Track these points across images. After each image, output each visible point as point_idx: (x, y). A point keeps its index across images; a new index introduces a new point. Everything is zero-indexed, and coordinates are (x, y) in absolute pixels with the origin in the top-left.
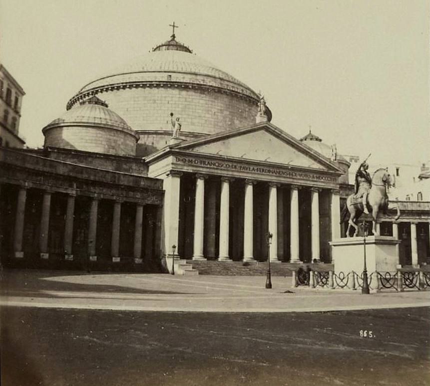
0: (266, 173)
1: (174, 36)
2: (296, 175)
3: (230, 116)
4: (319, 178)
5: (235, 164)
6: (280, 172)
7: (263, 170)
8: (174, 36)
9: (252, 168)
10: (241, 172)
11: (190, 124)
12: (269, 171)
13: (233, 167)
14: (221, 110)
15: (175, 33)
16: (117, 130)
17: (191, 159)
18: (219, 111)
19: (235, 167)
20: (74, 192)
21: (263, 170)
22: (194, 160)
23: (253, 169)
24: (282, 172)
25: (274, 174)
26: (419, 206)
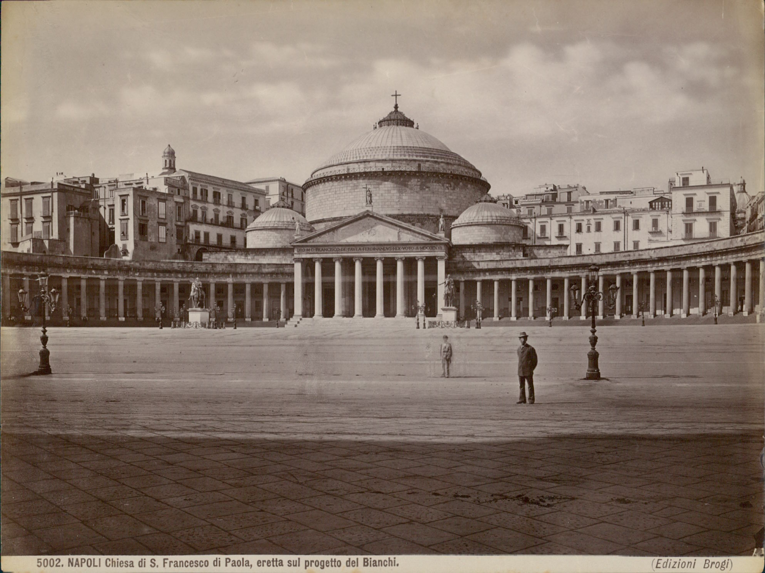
1: (396, 107)
2: (399, 248)
3: (398, 195)
4: (423, 248)
6: (384, 248)
7: (369, 249)
8: (396, 107)
9: (358, 248)
10: (349, 253)
11: (361, 208)
14: (388, 190)
15: (397, 103)
16: (282, 229)
17: (308, 248)
18: (387, 192)
20: (231, 280)
21: (369, 249)
22: (310, 248)
24: (387, 248)
25: (379, 251)
26: (523, 263)
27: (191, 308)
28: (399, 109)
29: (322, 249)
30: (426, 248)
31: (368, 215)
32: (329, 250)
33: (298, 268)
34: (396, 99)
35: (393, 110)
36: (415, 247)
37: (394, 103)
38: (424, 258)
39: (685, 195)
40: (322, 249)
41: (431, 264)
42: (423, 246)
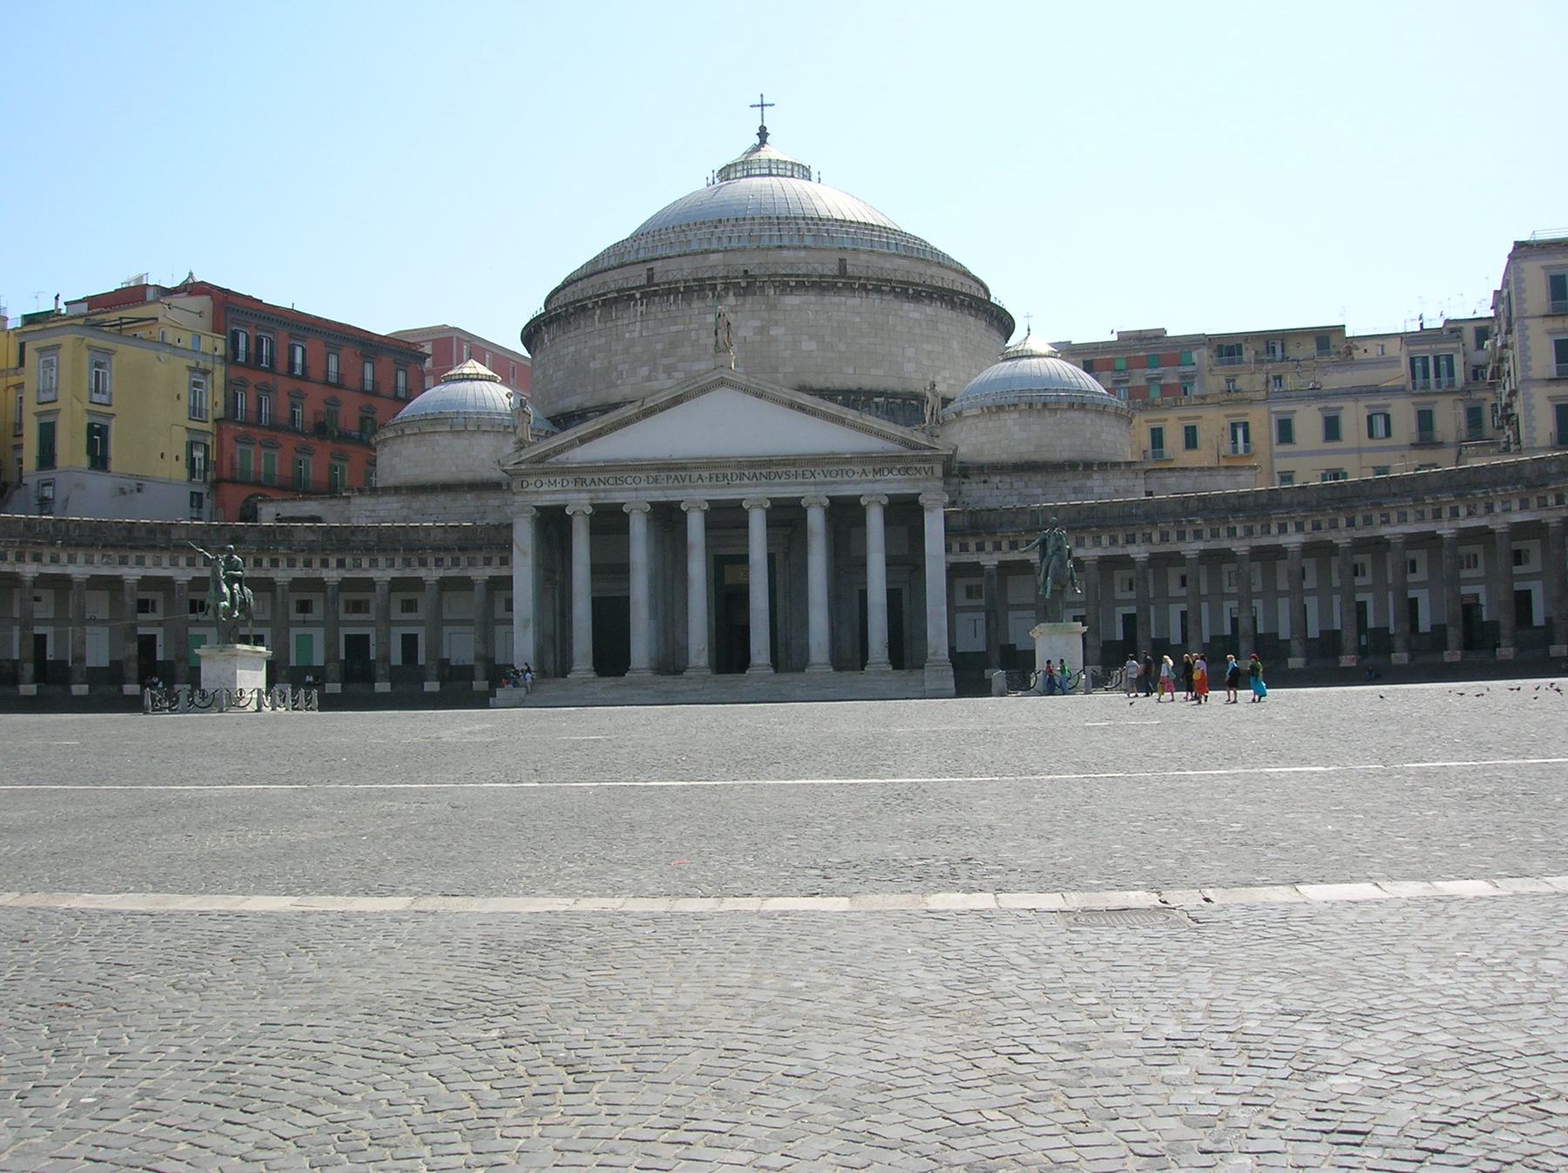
1: (763, 134)
4: (881, 471)
5: (654, 474)
8: (763, 134)
13: (651, 480)
19: (656, 480)
21: (725, 476)
22: (559, 480)
30: (890, 472)
31: (722, 383)
32: (611, 481)
33: (524, 535)
34: (762, 115)
35: (757, 141)
36: (858, 469)
38: (885, 501)
41: (904, 514)
42: (878, 463)
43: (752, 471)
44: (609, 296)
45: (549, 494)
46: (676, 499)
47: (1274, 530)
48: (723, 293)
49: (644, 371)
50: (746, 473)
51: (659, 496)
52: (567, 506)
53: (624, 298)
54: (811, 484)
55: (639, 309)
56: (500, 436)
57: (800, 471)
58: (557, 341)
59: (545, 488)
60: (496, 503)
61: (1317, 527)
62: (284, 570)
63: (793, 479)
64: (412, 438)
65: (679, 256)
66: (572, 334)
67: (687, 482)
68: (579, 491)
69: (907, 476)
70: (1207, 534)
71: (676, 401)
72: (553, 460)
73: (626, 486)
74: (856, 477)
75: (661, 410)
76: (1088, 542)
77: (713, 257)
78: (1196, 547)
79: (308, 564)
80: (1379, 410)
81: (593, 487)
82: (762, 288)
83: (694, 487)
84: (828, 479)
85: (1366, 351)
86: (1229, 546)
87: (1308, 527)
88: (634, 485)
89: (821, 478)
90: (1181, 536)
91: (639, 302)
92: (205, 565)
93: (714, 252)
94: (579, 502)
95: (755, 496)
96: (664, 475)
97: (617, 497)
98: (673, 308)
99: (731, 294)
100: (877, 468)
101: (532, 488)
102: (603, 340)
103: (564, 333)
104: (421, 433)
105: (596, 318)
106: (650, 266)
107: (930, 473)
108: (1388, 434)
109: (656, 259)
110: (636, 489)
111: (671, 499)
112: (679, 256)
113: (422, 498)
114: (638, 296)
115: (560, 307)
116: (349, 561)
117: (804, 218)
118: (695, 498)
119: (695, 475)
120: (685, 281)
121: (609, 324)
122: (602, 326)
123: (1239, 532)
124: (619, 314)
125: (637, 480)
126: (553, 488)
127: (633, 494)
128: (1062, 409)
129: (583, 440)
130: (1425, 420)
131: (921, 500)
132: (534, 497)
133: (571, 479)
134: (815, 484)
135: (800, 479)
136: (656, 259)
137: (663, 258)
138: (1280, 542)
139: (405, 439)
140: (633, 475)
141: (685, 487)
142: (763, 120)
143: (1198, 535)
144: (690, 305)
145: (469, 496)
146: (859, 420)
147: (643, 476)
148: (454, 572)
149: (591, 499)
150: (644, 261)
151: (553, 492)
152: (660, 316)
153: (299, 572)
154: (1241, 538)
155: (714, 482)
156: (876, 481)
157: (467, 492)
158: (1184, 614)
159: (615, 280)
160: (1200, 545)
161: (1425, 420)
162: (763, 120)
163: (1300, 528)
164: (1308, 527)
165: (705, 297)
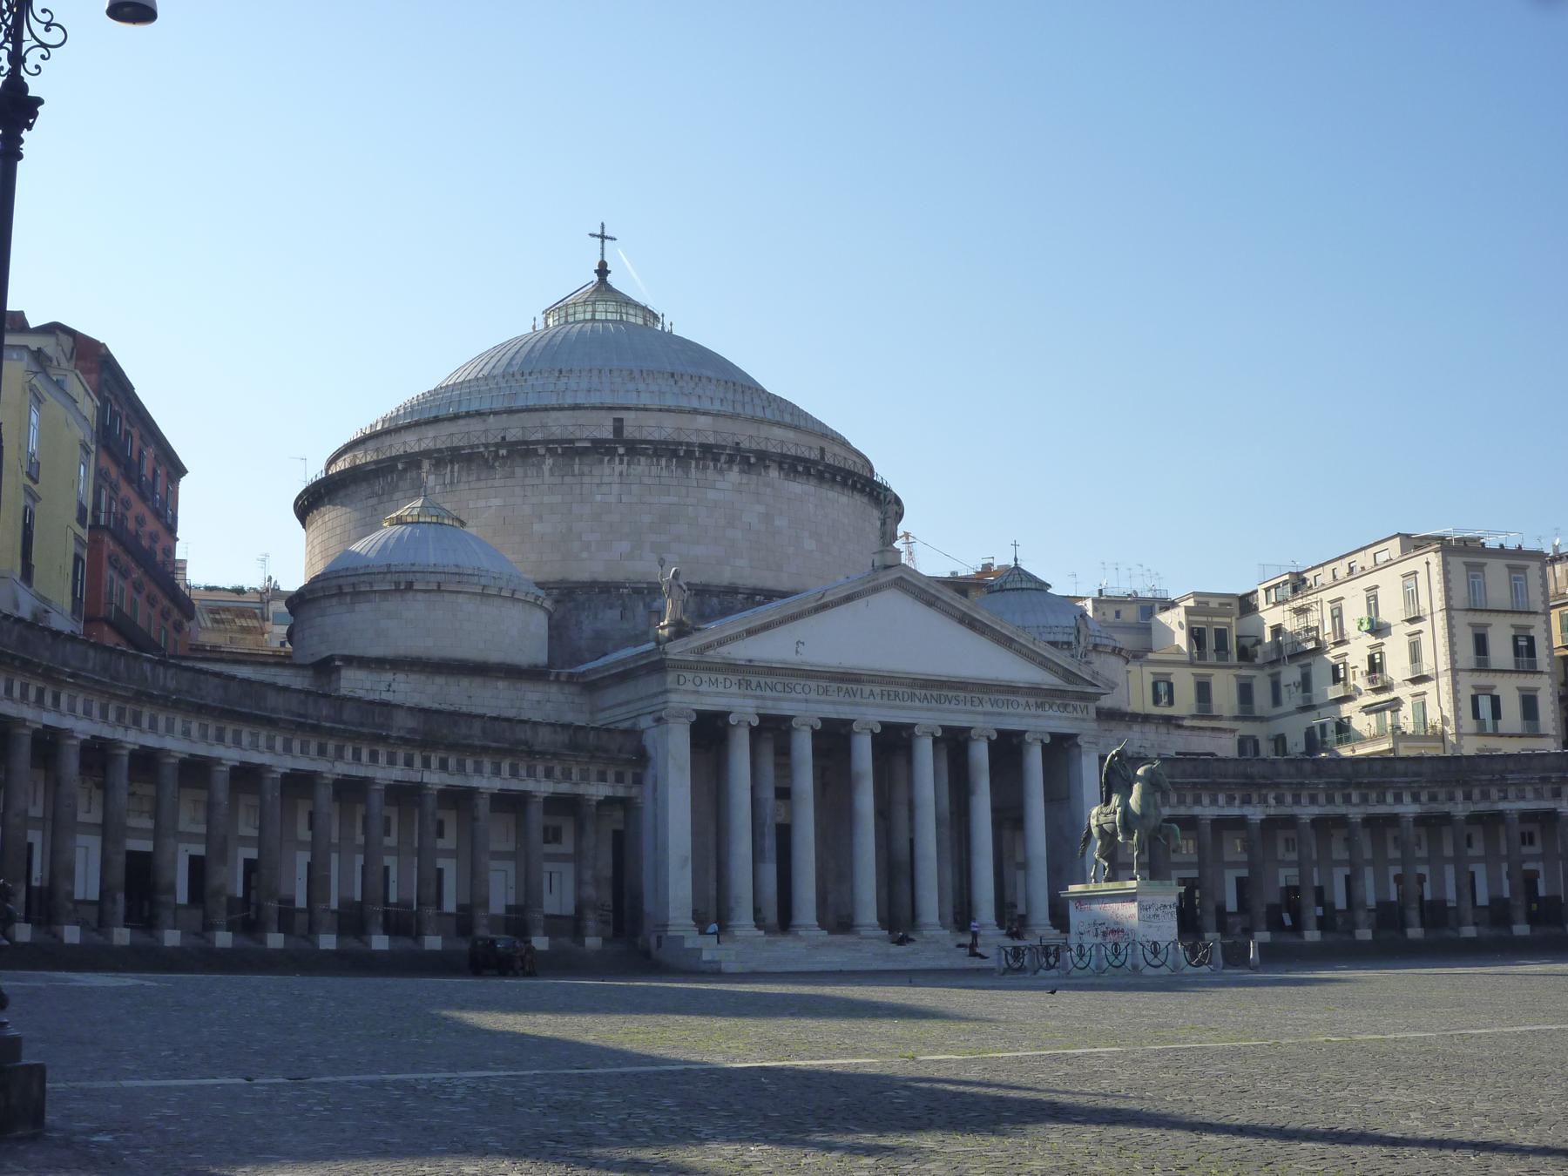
0: (902, 703)
1: (603, 271)
2: (981, 702)
5: (823, 684)
7: (896, 695)
8: (603, 271)
12: (912, 697)
13: (821, 691)
15: (606, 260)
21: (896, 695)
22: (721, 678)
23: (872, 693)
27: (1084, 881)
28: (609, 278)
29: (759, 685)
30: (1051, 707)
32: (779, 687)
34: (603, 248)
35: (596, 278)
36: (1022, 700)
37: (599, 259)
39: (1512, 626)
40: (759, 685)
43: (923, 692)
44: (577, 445)
45: (715, 696)
46: (789, 714)
47: (1390, 798)
48: (725, 466)
49: (624, 546)
50: (918, 695)
51: (832, 712)
52: (731, 713)
53: (600, 449)
54: (979, 713)
55: (618, 468)
56: (527, 606)
57: (969, 696)
58: (462, 486)
59: (704, 688)
60: (535, 696)
61: (1433, 798)
62: (384, 768)
63: (961, 707)
64: (420, 596)
65: (660, 410)
66: (497, 483)
67: (858, 699)
68: (745, 696)
69: (1065, 714)
70: (1322, 798)
71: (849, 598)
72: (711, 652)
73: (794, 695)
74: (1020, 710)
75: (833, 607)
76: (1206, 800)
77: (702, 421)
78: (1312, 812)
79: (409, 763)
80: (1164, 678)
81: (758, 692)
82: (766, 467)
83: (867, 705)
84: (996, 709)
85: (1104, 614)
86: (1344, 812)
87: (1424, 797)
88: (803, 696)
89: (988, 707)
90: (1297, 800)
91: (617, 459)
92: (302, 752)
93: (705, 413)
94: (743, 706)
95: (927, 718)
96: (834, 685)
97: (785, 708)
98: (665, 473)
99: (736, 468)
100: (1039, 701)
101: (690, 686)
102: (557, 499)
103: (479, 479)
104: (439, 590)
105: (546, 468)
106: (618, 415)
107: (1085, 712)
108: (1171, 702)
109: (628, 409)
110: (807, 701)
111: (843, 717)
112: (660, 410)
113: (440, 680)
114: (621, 450)
115: (486, 446)
116: (452, 762)
117: (749, 388)
118: (869, 714)
119: (867, 689)
120: (688, 444)
121: (568, 479)
122: (558, 480)
123: (1355, 798)
124: (586, 469)
125: (807, 690)
126: (713, 688)
127: (803, 706)
128: (1106, 653)
129: (751, 632)
130: (1203, 690)
131: (1079, 740)
132: (692, 698)
133: (735, 679)
134: (985, 714)
135: (968, 706)
136: (628, 409)
137: (637, 409)
138: (1396, 811)
139: (410, 595)
140: (803, 683)
141: (857, 704)
142: (602, 255)
143: (1313, 800)
144: (687, 472)
145: (501, 684)
146: (1031, 646)
147: (813, 684)
148: (564, 788)
149: (757, 707)
150: (610, 408)
151: (718, 694)
152: (646, 480)
153: (398, 773)
154: (1355, 805)
155: (885, 697)
156: (1039, 716)
157: (499, 678)
158: (1348, 878)
159: (559, 426)
160: (1316, 810)
161: (1203, 690)
162: (602, 255)
163: (1416, 799)
164: (1424, 797)
165: (705, 468)
